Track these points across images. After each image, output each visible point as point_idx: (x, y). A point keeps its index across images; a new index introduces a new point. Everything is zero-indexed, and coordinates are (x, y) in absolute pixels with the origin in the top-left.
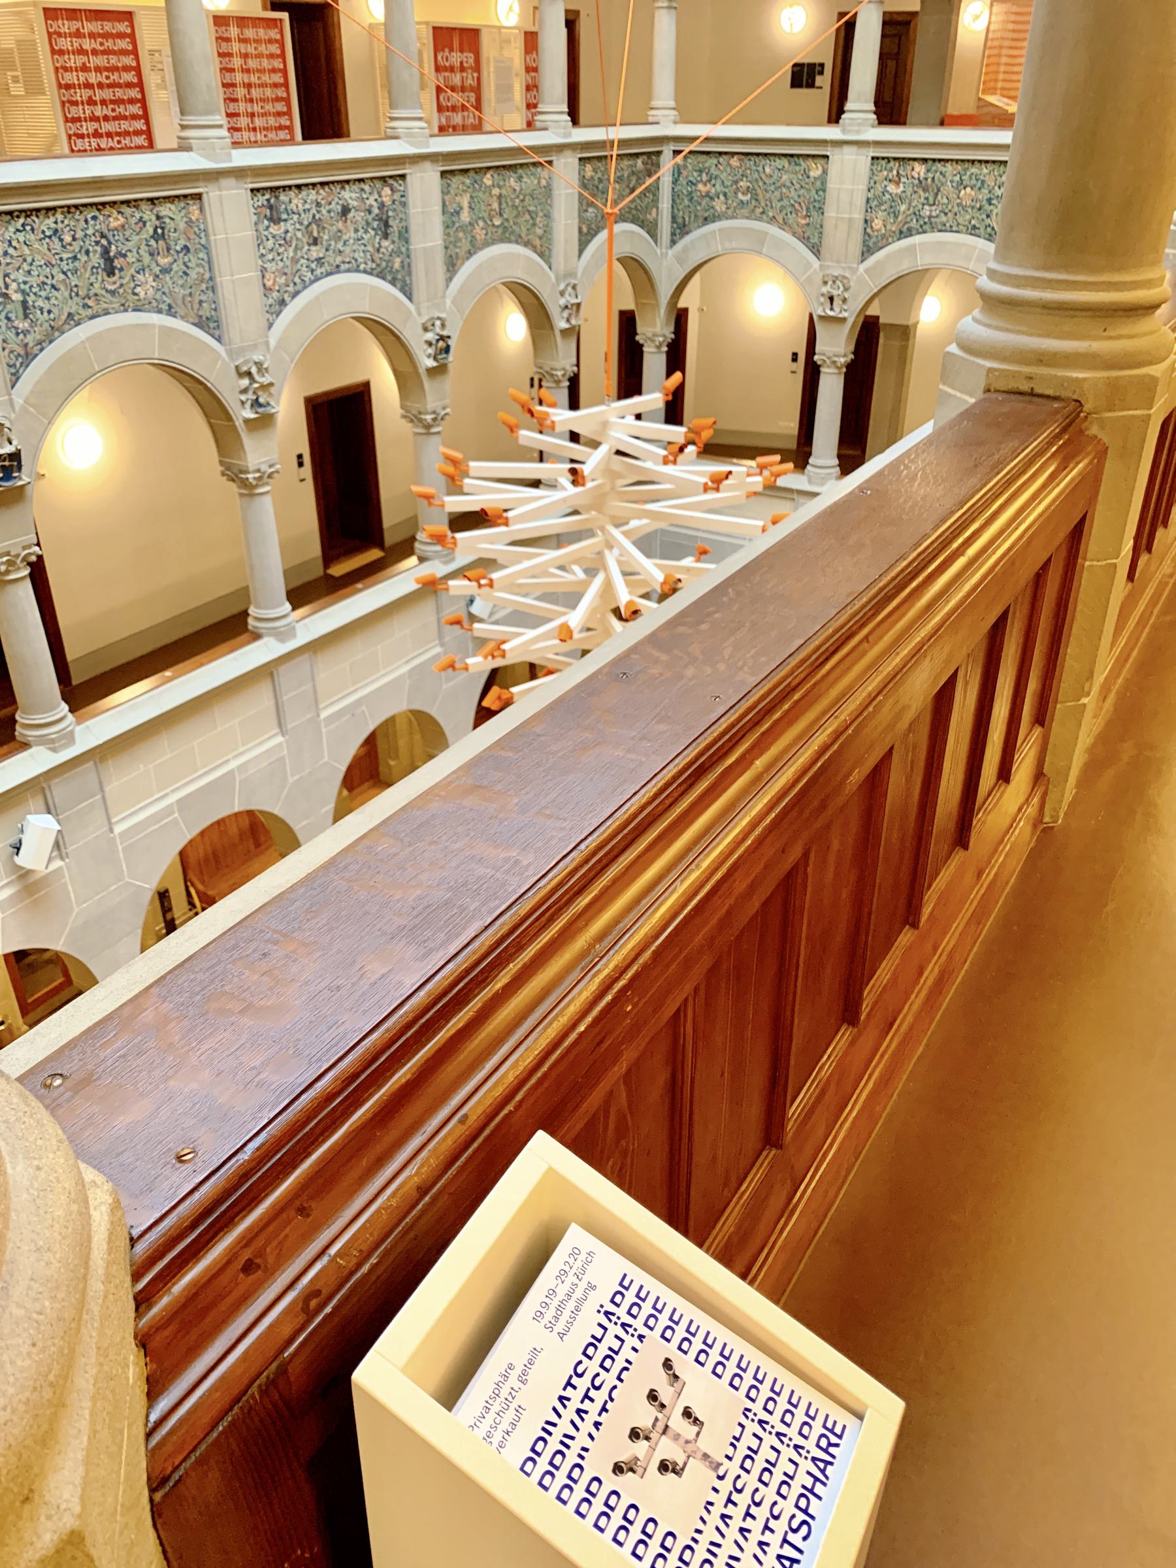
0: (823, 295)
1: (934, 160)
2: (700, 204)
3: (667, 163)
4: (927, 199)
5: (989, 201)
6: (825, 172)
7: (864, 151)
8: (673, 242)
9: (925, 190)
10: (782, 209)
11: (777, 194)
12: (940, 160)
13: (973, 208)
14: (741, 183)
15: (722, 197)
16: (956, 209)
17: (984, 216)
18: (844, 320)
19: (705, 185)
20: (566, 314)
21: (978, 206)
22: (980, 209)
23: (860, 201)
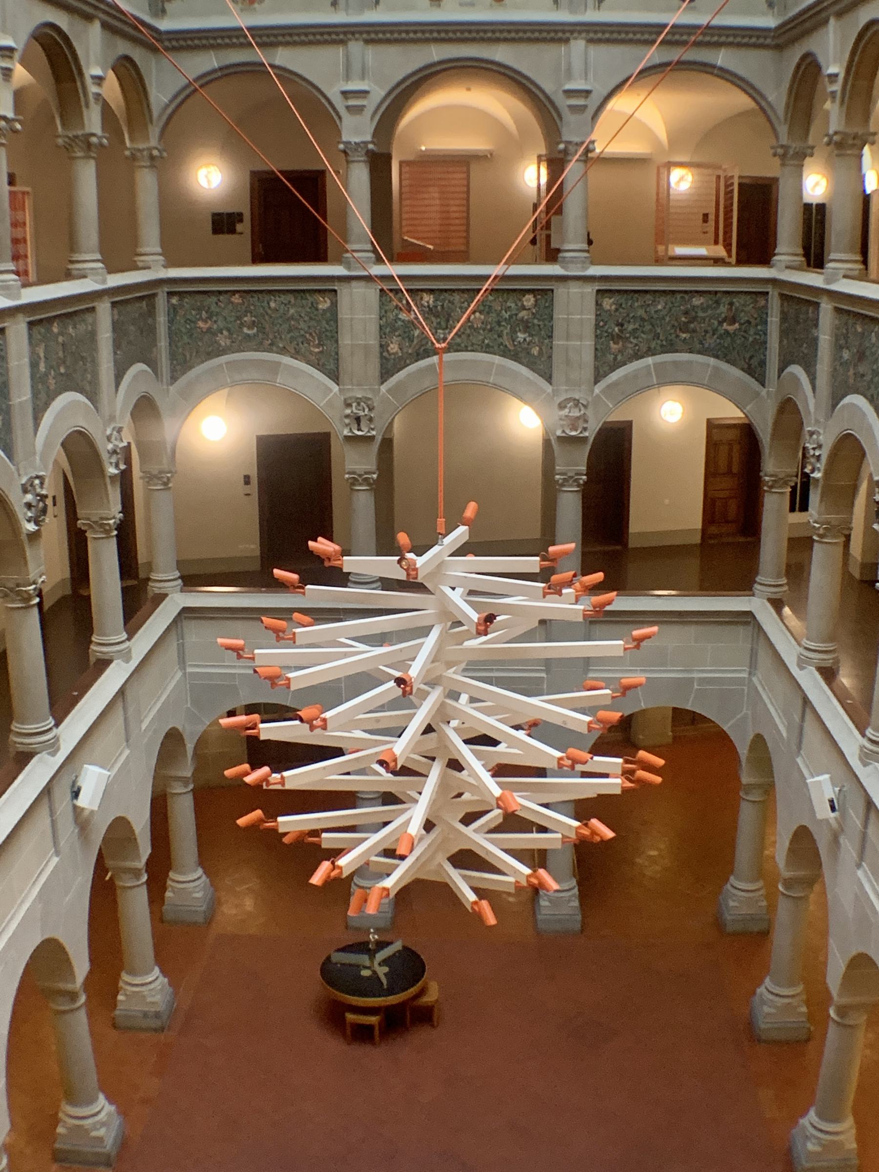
0: (347, 416)
1: (441, 290)
2: (201, 340)
3: (161, 302)
4: (439, 323)
5: (499, 323)
6: (334, 304)
7: (370, 284)
8: (174, 379)
9: (437, 316)
10: (292, 339)
11: (286, 326)
12: (446, 290)
13: (484, 330)
14: (245, 319)
15: (225, 333)
16: (468, 331)
17: (496, 336)
18: (372, 438)
19: (206, 322)
20: (114, 460)
21: (489, 327)
22: (491, 330)
23: (373, 328)
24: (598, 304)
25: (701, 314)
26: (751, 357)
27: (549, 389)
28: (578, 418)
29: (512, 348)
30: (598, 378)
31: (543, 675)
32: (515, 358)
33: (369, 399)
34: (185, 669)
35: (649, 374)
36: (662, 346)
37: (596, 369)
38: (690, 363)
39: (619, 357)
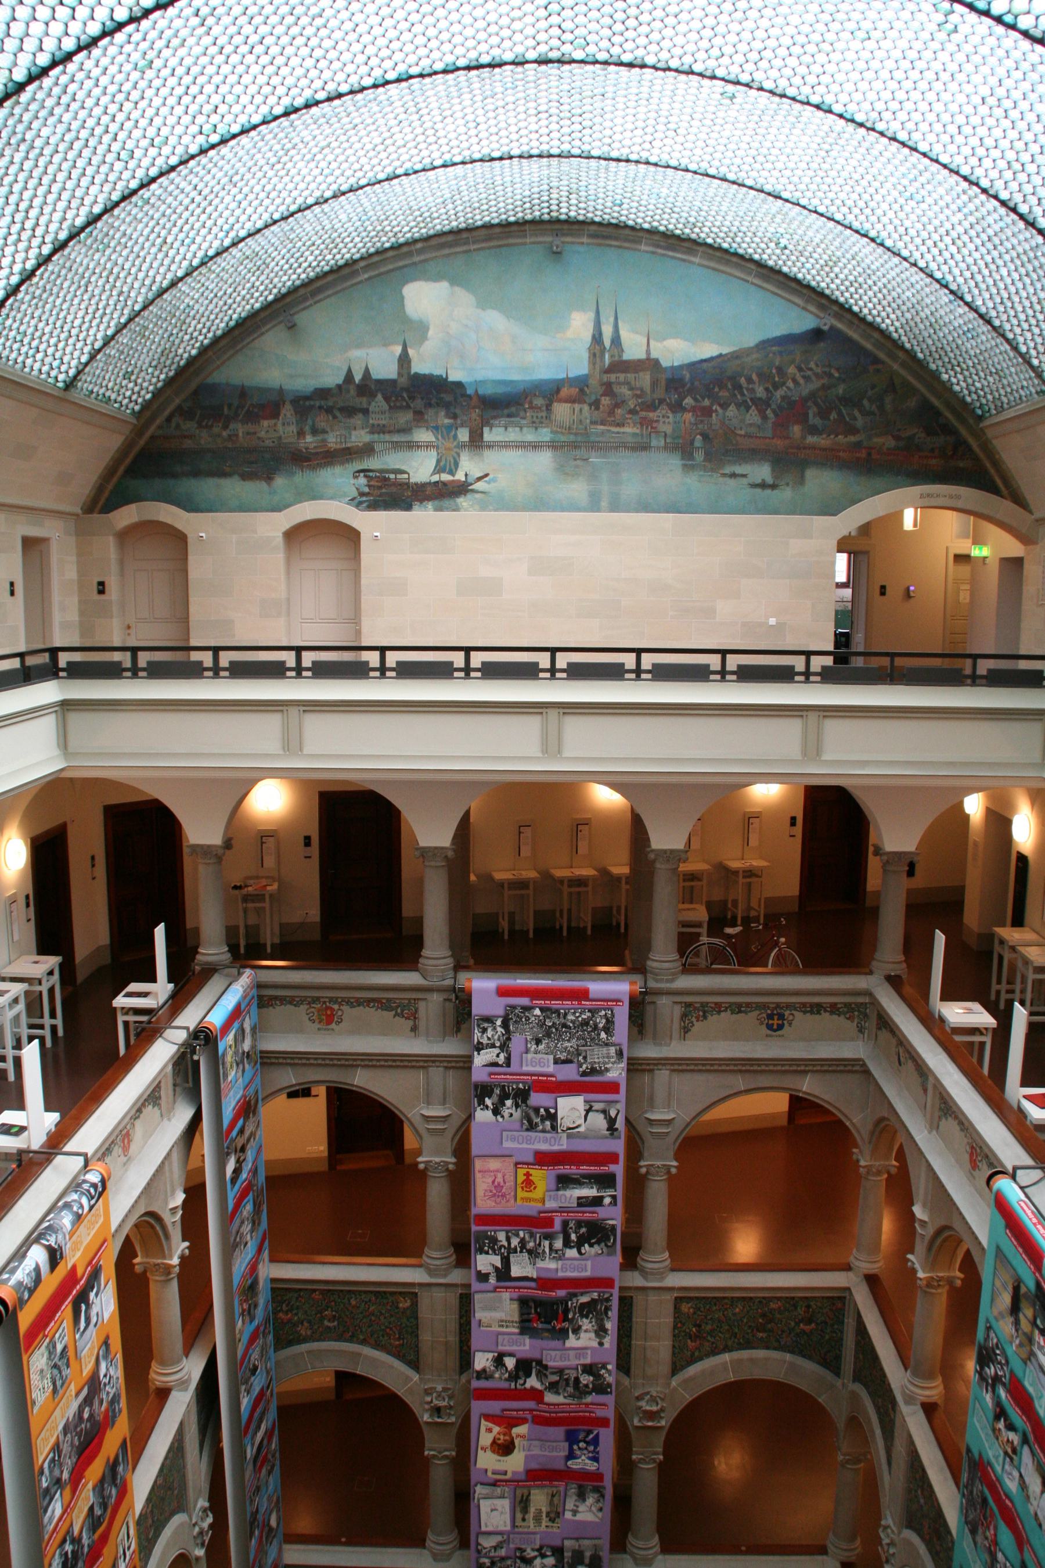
6: (415, 1304)
15: (306, 1324)
24: (676, 1308)
25: (778, 1316)
30: (675, 1370)
35: (726, 1369)
37: (674, 1363)
38: (767, 1359)
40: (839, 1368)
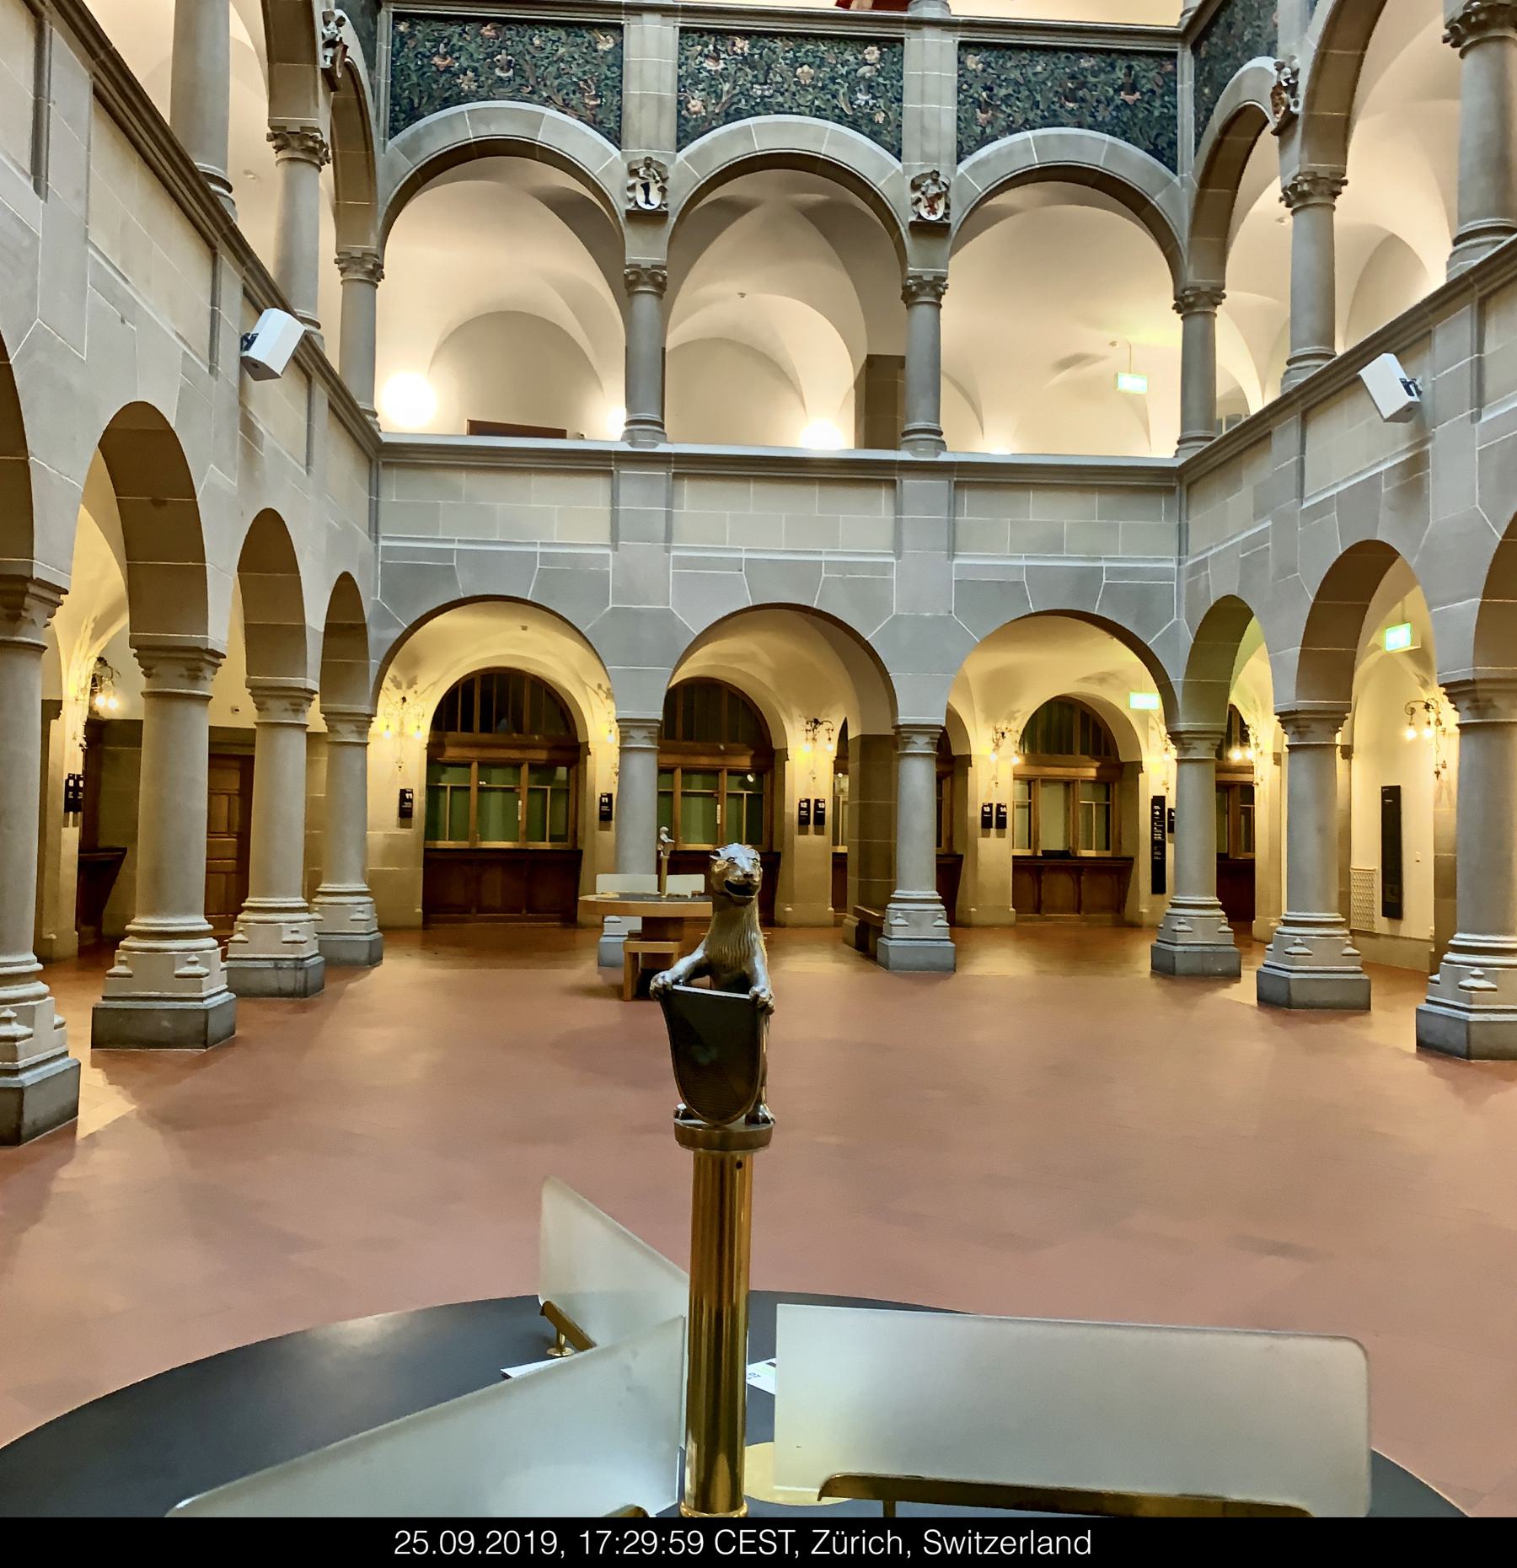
26: (1158, 136)
27: (899, 166)
28: (938, 196)
29: (850, 113)
31: (892, 560)
32: (854, 125)
33: (662, 165)
34: (377, 541)
35: (1028, 150)
36: (1044, 117)
39: (988, 130)
40: (1175, 160)
